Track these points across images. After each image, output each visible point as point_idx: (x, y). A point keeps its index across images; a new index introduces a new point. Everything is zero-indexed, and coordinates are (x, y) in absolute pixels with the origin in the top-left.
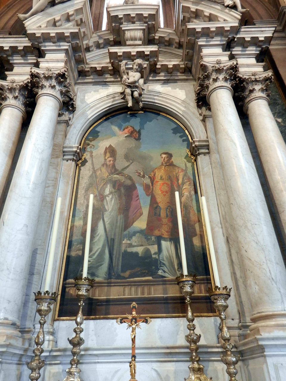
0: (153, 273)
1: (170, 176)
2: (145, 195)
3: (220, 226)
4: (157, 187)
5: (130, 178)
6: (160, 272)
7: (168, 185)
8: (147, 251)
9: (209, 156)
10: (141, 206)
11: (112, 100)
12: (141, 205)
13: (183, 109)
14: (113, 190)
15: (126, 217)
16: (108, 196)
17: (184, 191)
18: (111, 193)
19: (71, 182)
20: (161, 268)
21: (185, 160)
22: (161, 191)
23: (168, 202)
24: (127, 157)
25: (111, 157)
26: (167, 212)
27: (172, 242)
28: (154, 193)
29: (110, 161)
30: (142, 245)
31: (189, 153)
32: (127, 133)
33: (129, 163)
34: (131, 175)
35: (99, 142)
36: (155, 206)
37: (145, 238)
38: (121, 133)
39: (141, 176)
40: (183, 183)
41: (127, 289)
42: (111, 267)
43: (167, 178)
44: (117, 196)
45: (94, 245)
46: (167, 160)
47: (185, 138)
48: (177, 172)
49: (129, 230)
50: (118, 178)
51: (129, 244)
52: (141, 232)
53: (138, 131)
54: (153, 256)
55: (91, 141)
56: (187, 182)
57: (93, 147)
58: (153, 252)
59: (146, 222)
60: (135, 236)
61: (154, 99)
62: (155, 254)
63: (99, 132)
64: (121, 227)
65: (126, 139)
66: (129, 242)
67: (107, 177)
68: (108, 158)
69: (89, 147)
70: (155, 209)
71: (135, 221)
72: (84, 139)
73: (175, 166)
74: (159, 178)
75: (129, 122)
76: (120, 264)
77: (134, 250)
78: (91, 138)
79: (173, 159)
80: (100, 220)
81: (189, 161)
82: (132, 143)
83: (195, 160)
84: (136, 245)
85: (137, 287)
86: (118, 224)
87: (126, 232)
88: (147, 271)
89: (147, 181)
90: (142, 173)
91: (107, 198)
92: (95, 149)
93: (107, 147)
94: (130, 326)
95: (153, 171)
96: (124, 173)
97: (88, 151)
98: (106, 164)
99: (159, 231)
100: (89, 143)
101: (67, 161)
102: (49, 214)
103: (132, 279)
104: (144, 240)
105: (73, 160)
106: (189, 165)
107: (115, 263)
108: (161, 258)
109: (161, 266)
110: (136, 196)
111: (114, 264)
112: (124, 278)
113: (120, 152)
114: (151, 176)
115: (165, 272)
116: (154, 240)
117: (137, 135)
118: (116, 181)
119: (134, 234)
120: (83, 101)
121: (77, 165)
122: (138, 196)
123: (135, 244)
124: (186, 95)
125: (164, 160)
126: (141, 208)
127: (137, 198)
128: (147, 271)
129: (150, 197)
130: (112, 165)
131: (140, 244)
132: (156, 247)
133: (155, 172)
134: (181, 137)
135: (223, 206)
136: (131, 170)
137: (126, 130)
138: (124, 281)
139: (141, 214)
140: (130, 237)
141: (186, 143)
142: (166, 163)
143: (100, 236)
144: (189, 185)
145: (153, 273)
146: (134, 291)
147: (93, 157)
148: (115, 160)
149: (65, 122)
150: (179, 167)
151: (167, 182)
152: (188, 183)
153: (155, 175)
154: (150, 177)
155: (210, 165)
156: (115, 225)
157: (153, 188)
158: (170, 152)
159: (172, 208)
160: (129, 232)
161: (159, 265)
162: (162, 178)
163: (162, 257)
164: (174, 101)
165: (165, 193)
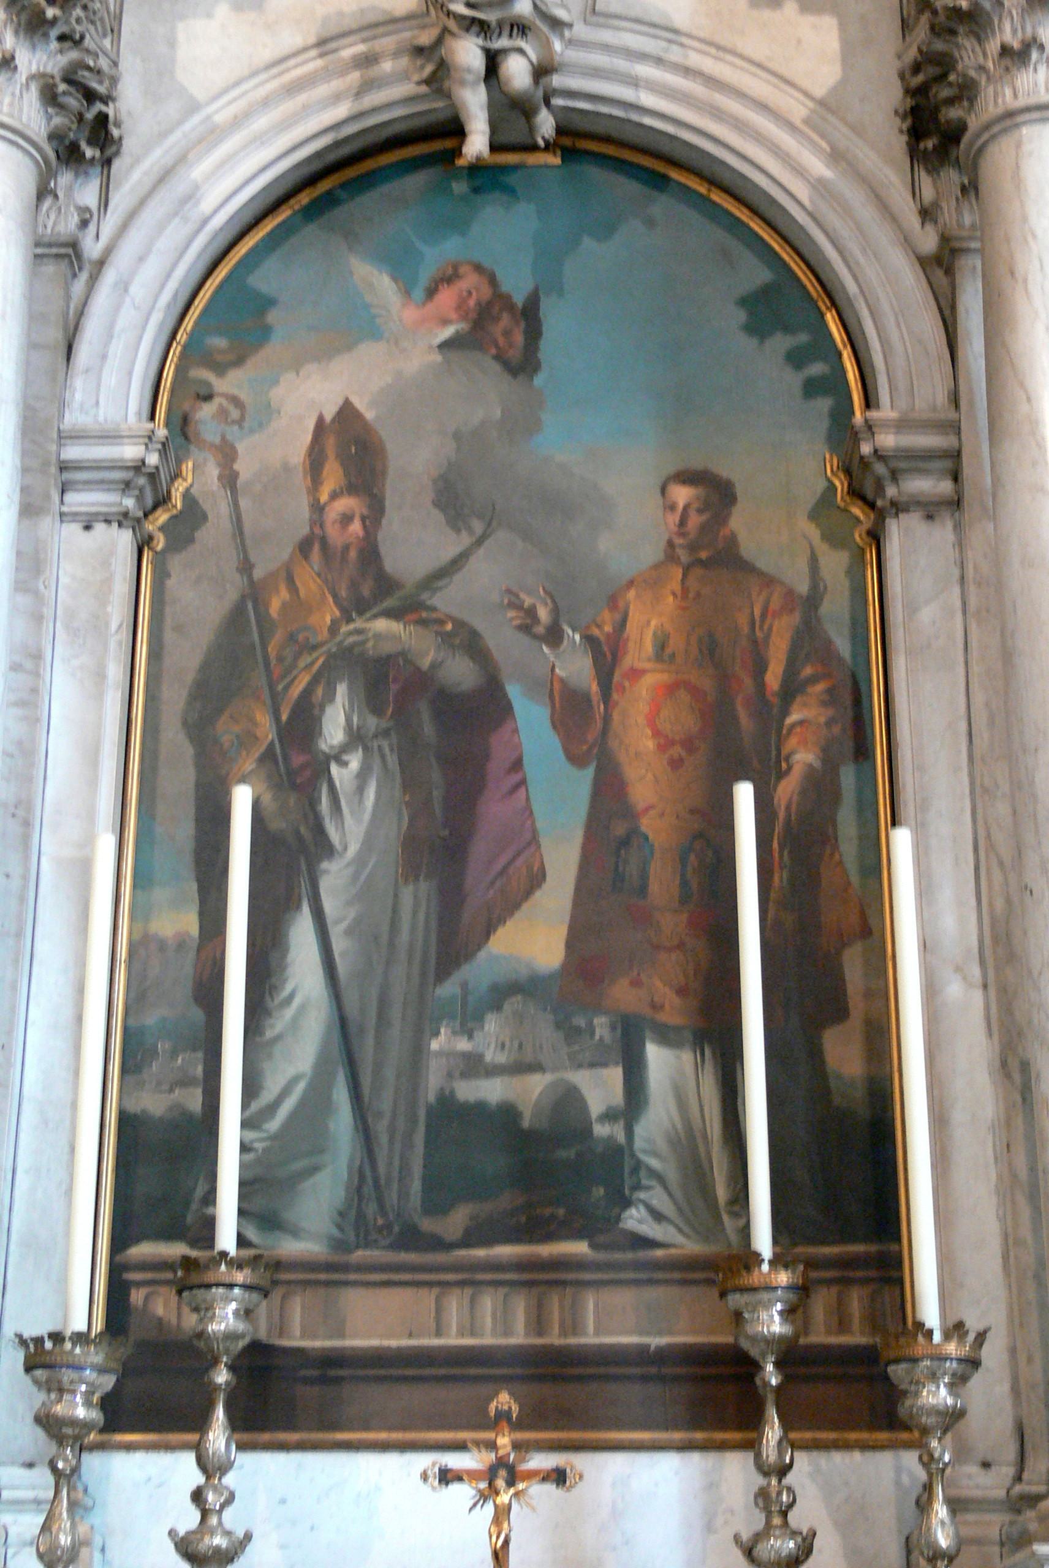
0: (596, 1225)
2: (561, 753)
3: (976, 971)
5: (471, 643)
6: (635, 1219)
7: (695, 691)
8: (569, 1100)
9: (958, 527)
11: (355, 77)
13: (819, 167)
14: (372, 723)
15: (451, 898)
16: (338, 756)
17: (792, 742)
18: (356, 738)
19: (116, 672)
20: (642, 1195)
21: (813, 532)
22: (656, 733)
24: (452, 499)
25: (351, 488)
26: (683, 875)
27: (708, 1052)
28: (613, 744)
29: (346, 519)
31: (840, 485)
33: (466, 540)
34: (479, 623)
35: (276, 382)
36: (620, 829)
37: (558, 1026)
38: (411, 314)
39: (540, 630)
40: (791, 690)
41: (455, 1305)
42: (365, 1183)
44: (392, 760)
45: (270, 1056)
46: (703, 528)
47: (817, 369)
48: (757, 612)
53: (520, 305)
54: (601, 1130)
55: (220, 369)
56: (813, 680)
57: (235, 414)
58: (596, 1105)
59: (562, 932)
61: (635, 82)
62: (609, 1116)
63: (269, 302)
64: (418, 955)
66: (463, 1045)
67: (333, 629)
68: (334, 496)
69: (206, 412)
70: (618, 850)
71: (502, 920)
72: (176, 350)
73: (746, 567)
74: (649, 647)
75: (463, 234)
77: (492, 1091)
78: (219, 342)
79: (738, 522)
80: (298, 907)
81: (833, 539)
82: (484, 395)
83: (876, 537)
85: (506, 1296)
86: (404, 937)
87: (449, 989)
88: (561, 1212)
89: (575, 666)
90: (543, 614)
91: (334, 769)
92: (252, 431)
93: (328, 417)
94: (483, 1497)
95: (613, 602)
96: (434, 609)
97: (202, 444)
98: (324, 542)
99: (636, 983)
100: (208, 385)
101: (88, 528)
102: (16, 883)
103: (481, 1253)
105: (123, 519)
106: (835, 564)
107: (390, 1164)
108: (639, 1144)
111: (382, 1169)
112: (439, 1244)
113: (413, 461)
114: (596, 632)
117: (519, 338)
120: (162, 73)
121: (142, 545)
122: (517, 765)
124: (848, 53)
125: (683, 522)
126: (534, 840)
127: (515, 778)
128: (561, 1212)
129: (590, 772)
130: (361, 551)
132: (615, 1075)
133: (621, 604)
134: (796, 359)
135: (1001, 864)
136: (481, 589)
137: (447, 297)
138: (440, 1258)
139: (537, 879)
140: (468, 1022)
141: (824, 404)
142: (693, 548)
143: (303, 1008)
144: (824, 704)
145: (596, 1225)
146: (494, 1315)
149: (57, 256)
150: (769, 581)
154: (590, 640)
155: (956, 590)
156: (384, 938)
157: (607, 719)
158: (723, 470)
160: (464, 986)
161: (628, 1183)
164: (763, 107)
165: (677, 751)
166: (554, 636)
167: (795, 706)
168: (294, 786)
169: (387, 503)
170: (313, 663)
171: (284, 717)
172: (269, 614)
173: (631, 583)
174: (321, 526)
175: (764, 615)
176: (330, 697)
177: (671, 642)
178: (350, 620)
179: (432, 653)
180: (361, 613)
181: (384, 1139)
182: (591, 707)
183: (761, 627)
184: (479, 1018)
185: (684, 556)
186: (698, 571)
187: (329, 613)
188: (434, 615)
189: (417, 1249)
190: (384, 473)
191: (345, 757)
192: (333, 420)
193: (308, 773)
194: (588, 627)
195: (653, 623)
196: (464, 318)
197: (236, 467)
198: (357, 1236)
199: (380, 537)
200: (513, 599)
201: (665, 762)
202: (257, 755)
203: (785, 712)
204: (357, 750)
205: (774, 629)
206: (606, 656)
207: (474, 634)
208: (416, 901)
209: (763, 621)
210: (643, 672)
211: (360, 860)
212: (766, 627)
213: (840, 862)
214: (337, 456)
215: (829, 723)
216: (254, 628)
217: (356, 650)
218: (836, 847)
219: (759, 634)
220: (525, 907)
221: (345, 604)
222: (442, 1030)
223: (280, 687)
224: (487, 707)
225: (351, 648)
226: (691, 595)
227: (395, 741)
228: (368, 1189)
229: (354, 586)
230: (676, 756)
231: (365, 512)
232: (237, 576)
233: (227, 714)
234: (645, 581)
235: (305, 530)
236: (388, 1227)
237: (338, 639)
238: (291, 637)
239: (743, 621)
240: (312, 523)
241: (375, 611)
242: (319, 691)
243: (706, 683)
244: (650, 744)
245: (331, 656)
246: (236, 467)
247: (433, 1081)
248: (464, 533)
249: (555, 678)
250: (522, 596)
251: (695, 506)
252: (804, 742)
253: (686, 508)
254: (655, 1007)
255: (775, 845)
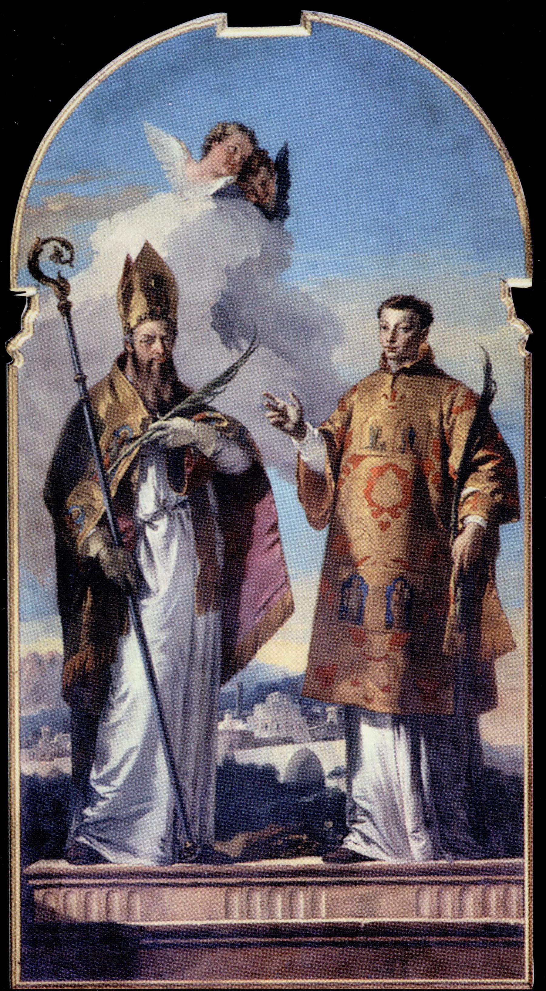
1: (412, 430)
4: (354, 487)
6: (353, 843)
8: (309, 762)
10: (286, 577)
12: (290, 572)
14: (175, 497)
17: (466, 509)
18: (163, 508)
20: (357, 826)
22: (372, 504)
23: (395, 561)
24: (226, 321)
25: (152, 315)
26: (388, 608)
28: (340, 511)
29: (150, 339)
30: (288, 741)
32: (224, 170)
33: (236, 356)
37: (304, 712)
38: (193, 169)
39: (289, 426)
40: (469, 467)
41: (237, 898)
42: (179, 817)
43: (399, 441)
44: (189, 526)
48: (445, 408)
49: (241, 676)
50: (189, 433)
51: (242, 733)
52: (287, 687)
54: (330, 783)
56: (484, 460)
58: (327, 767)
60: (263, 701)
62: (336, 774)
64: (208, 667)
65: (220, 209)
66: (240, 726)
67: (144, 426)
68: (141, 321)
70: (343, 591)
71: (265, 640)
74: (367, 440)
76: (211, 809)
77: (259, 757)
79: (434, 338)
80: (128, 630)
84: (267, 740)
86: (199, 652)
87: (230, 687)
88: (305, 837)
90: (292, 414)
91: (149, 531)
93: (134, 258)
95: (342, 404)
98: (134, 356)
103: (253, 865)
104: (297, 719)
107: (193, 806)
108: (356, 792)
109: (355, 821)
110: (268, 527)
111: (188, 810)
112: (225, 859)
114: (329, 427)
115: (367, 840)
116: (336, 722)
118: (182, 450)
119: (262, 692)
122: (274, 527)
123: (265, 735)
125: (393, 341)
126: (286, 582)
128: (305, 837)
131: (283, 734)
132: (340, 745)
137: (218, 152)
138: (226, 868)
139: (288, 610)
140: (244, 709)
142: (400, 359)
143: (134, 701)
144: (491, 479)
147: (73, 310)
148: (172, 331)
150: (455, 384)
151: (398, 461)
152: (490, 465)
153: (348, 422)
154: (324, 433)
157: (337, 492)
159: (411, 592)
160: (240, 685)
161: (349, 818)
162: (377, 437)
163: (360, 786)
166: (299, 430)
167: (469, 482)
168: (121, 545)
169: (179, 326)
170: (130, 453)
171: (113, 494)
172: (98, 416)
173: (355, 389)
174: (133, 347)
175: (450, 412)
176: (143, 478)
177: (383, 435)
178: (156, 420)
179: (214, 443)
180: (163, 414)
181: (189, 790)
182: (325, 484)
183: (448, 420)
184: (250, 707)
185: (394, 366)
186: (403, 377)
187: (142, 413)
188: (215, 415)
189: (213, 862)
190: (176, 301)
191: (156, 523)
192: (137, 259)
193: (131, 534)
194: (323, 424)
195: (371, 419)
196: (231, 172)
197: (69, 298)
198: (174, 852)
199: (174, 352)
200: (272, 403)
201: (377, 524)
202: (96, 522)
203: (462, 487)
204: (163, 516)
205: (457, 424)
206: (337, 446)
207: (243, 430)
208: (207, 623)
209: (449, 417)
210: (363, 457)
211: (169, 598)
212: (451, 421)
213: (496, 597)
214: (141, 290)
215: (493, 494)
216: (89, 426)
217: (161, 443)
218: (494, 586)
219: (446, 427)
220: (280, 629)
221: (152, 406)
222: (226, 716)
223: (109, 472)
224: (252, 484)
225: (156, 441)
226: (398, 397)
227: (189, 510)
228: (181, 823)
229: (157, 392)
230: (385, 520)
231: (164, 334)
232: (75, 384)
233: (73, 493)
234: (364, 386)
235: (120, 350)
236: (194, 847)
237: (148, 433)
238: (115, 433)
239: (434, 417)
240: (126, 342)
241: (173, 411)
242: (136, 473)
243: (406, 463)
244: (367, 512)
245: (144, 446)
246: (69, 298)
247: (221, 750)
248: (234, 350)
249: (300, 462)
250: (278, 400)
251: (403, 325)
252: (474, 508)
253: (396, 326)
254: (369, 700)
255: (452, 585)
